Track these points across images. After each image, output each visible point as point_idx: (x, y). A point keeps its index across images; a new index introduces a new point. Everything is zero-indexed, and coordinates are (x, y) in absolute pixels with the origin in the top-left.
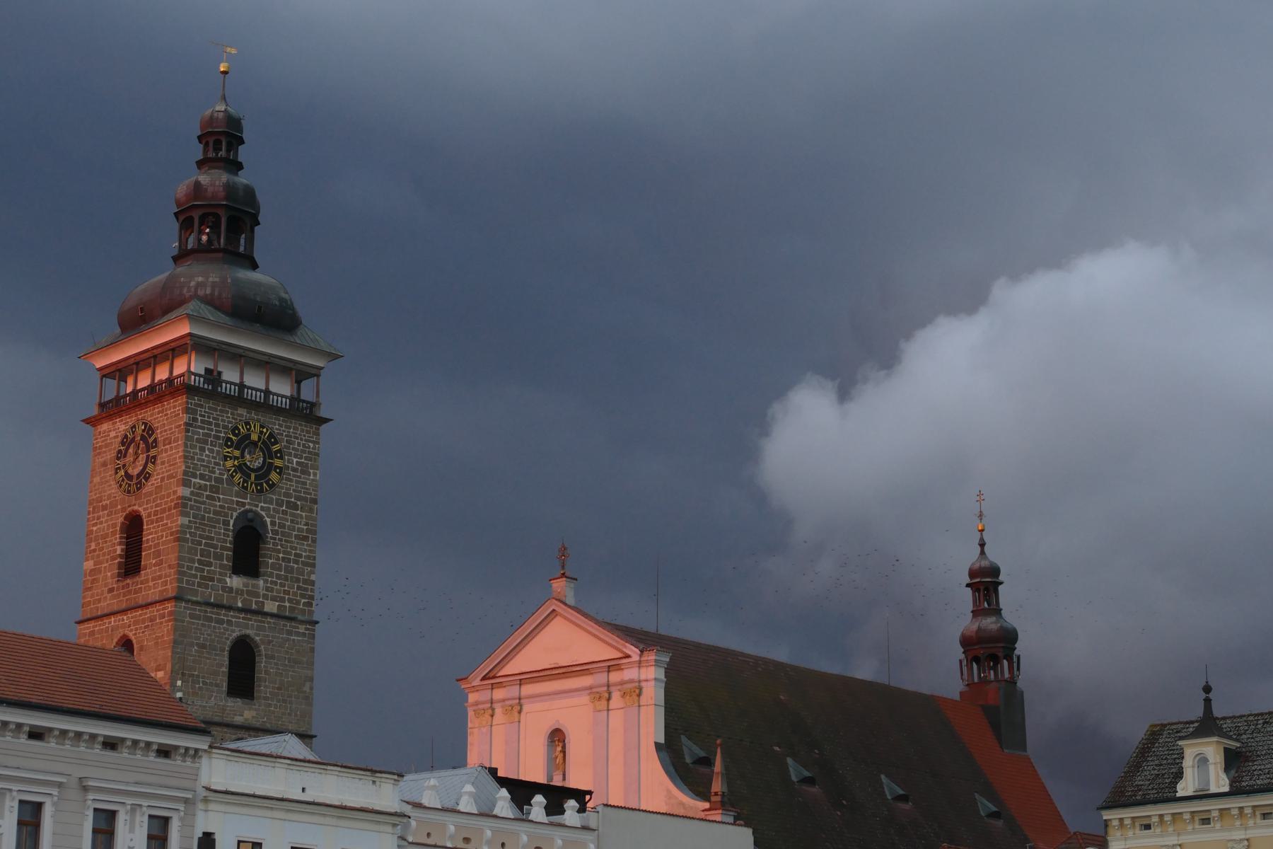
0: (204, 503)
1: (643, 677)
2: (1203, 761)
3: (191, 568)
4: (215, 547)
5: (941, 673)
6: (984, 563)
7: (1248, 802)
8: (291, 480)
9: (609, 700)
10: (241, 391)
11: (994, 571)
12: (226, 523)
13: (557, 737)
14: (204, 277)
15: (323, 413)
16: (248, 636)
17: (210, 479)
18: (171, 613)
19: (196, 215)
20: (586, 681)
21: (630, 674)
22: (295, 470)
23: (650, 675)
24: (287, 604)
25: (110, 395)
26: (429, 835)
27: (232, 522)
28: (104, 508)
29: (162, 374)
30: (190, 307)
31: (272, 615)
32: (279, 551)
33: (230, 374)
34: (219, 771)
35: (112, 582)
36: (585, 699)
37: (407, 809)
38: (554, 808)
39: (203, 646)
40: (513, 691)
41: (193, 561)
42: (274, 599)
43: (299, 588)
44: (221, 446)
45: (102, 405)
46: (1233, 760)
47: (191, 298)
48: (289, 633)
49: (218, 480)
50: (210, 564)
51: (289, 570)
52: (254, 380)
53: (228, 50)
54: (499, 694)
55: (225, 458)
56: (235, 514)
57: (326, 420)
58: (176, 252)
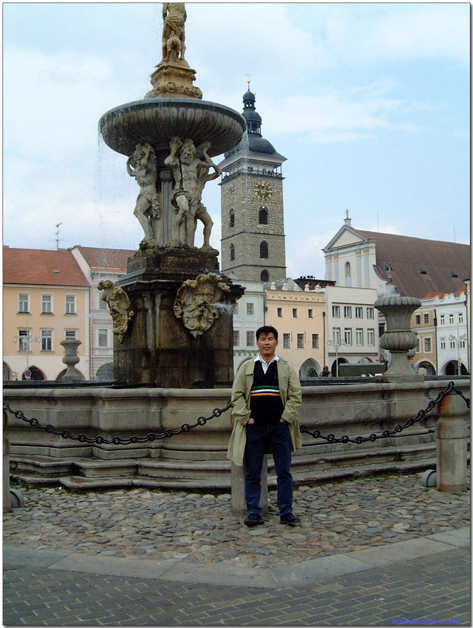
1: (369, 246)
9: (360, 253)
10: (258, 173)
12: (256, 210)
13: (348, 264)
15: (283, 177)
18: (242, 236)
20: (354, 248)
26: (273, 297)
28: (225, 208)
31: (272, 235)
36: (354, 253)
37: (266, 291)
38: (312, 288)
39: (252, 245)
40: (336, 252)
42: (272, 230)
48: (277, 239)
49: (253, 198)
50: (252, 222)
51: (276, 221)
54: (332, 253)
57: (284, 178)
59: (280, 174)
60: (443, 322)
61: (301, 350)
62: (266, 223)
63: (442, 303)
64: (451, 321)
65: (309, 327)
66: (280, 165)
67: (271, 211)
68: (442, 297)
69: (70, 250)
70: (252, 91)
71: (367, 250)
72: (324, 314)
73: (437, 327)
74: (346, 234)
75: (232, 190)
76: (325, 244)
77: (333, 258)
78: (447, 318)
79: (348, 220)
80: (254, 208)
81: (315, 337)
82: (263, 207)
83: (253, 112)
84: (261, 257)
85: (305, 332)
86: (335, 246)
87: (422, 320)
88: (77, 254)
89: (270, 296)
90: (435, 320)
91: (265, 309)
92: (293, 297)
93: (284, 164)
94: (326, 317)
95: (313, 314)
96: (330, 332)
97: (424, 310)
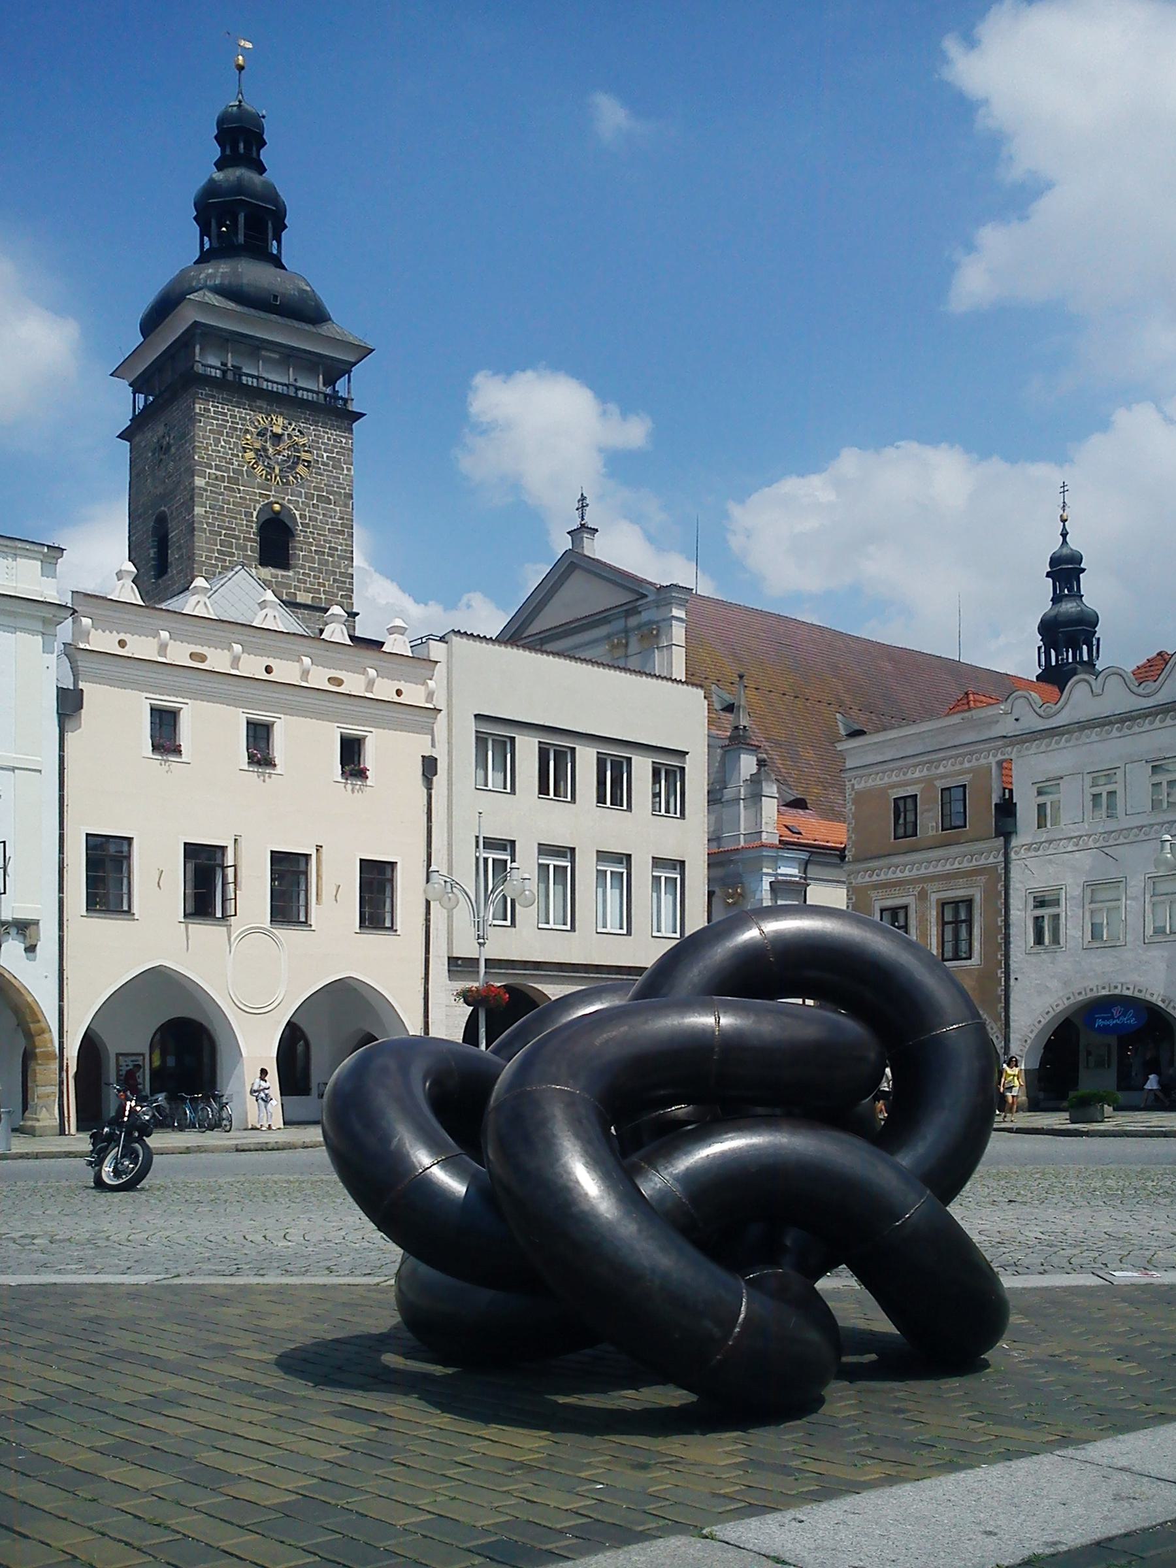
0: (222, 494)
3: (210, 558)
4: (237, 538)
6: (1065, 551)
8: (321, 475)
11: (1076, 559)
15: (354, 407)
17: (227, 470)
20: (603, 631)
21: (645, 616)
22: (324, 464)
24: (323, 596)
27: (255, 514)
28: (140, 516)
32: (311, 544)
41: (213, 551)
42: (307, 591)
43: (335, 580)
44: (238, 437)
47: (201, 289)
49: (237, 472)
53: (242, 43)
55: (244, 450)
56: (258, 506)
58: (197, 255)
61: (286, 934)
62: (286, 567)
66: (345, 369)
67: (307, 525)
73: (1014, 842)
80: (240, 505)
81: (376, 880)
82: (277, 507)
85: (319, 848)
87: (929, 822)
94: (439, 781)
95: (370, 758)
97: (942, 770)
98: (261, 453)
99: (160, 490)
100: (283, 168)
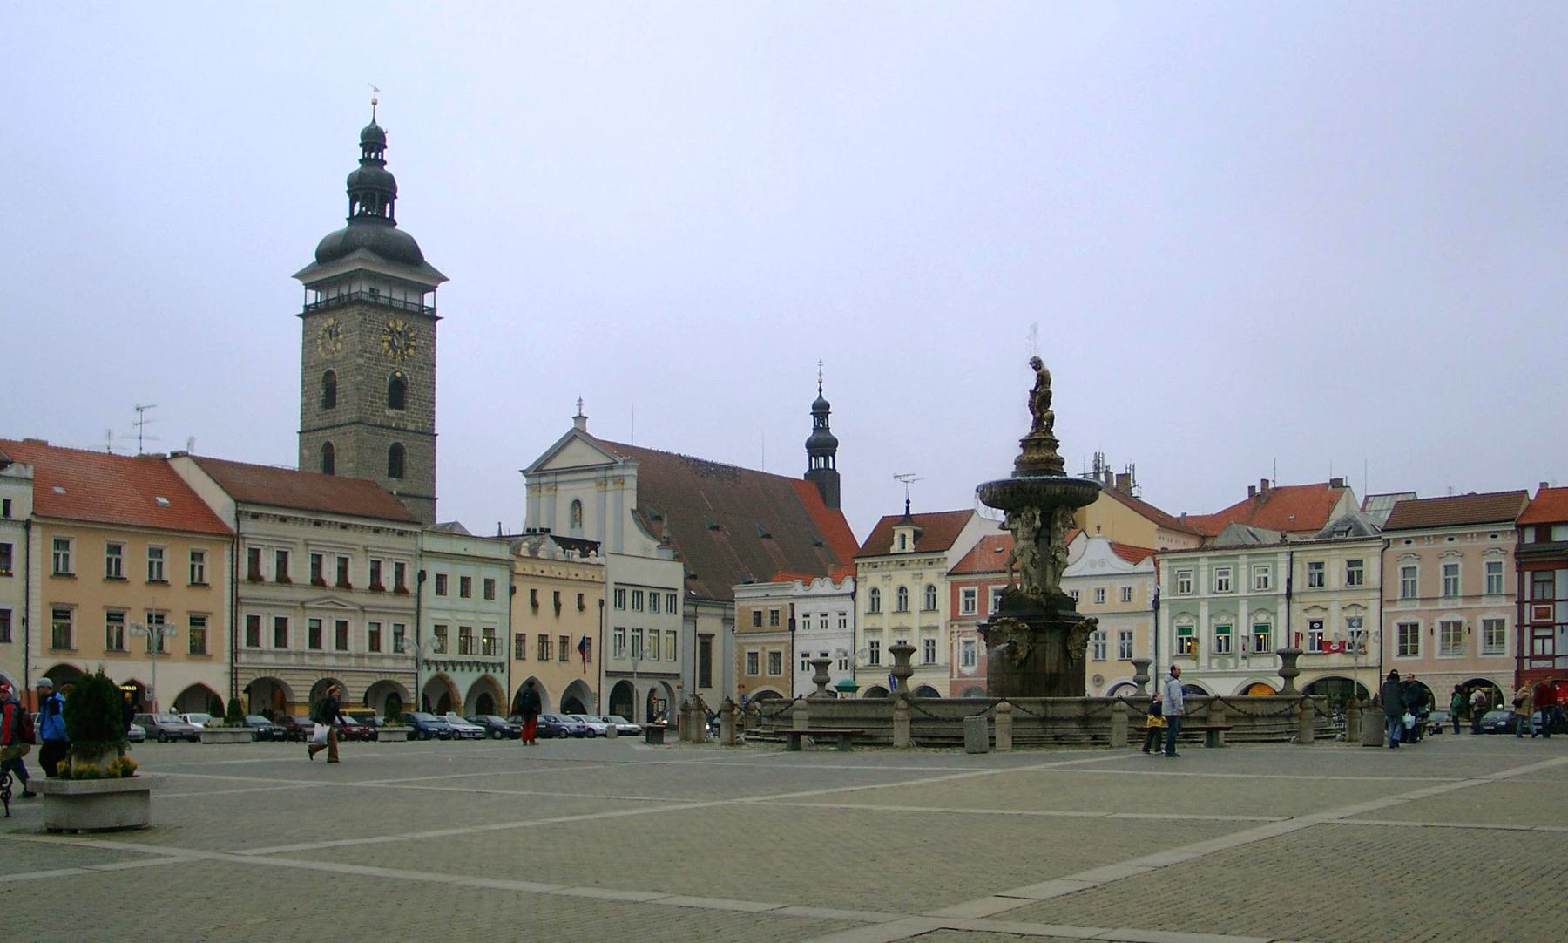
2: (903, 537)
5: (795, 465)
7: (923, 557)
13: (577, 504)
14: (367, 232)
16: (397, 444)
19: (360, 194)
20: (593, 475)
21: (617, 472)
23: (631, 473)
25: (311, 301)
29: (345, 291)
30: (359, 254)
33: (384, 292)
34: (430, 543)
35: (319, 411)
36: (592, 484)
38: (584, 554)
40: (551, 478)
45: (306, 307)
46: (917, 535)
52: (398, 296)
54: (544, 479)
59: (433, 309)
60: (807, 625)
62: (402, 408)
63: (812, 592)
64: (824, 624)
65: (576, 625)
66: (433, 289)
68: (807, 583)
69: (163, 459)
70: (379, 123)
71: (620, 481)
72: (602, 603)
74: (577, 446)
75: (332, 332)
76: (527, 463)
77: (544, 489)
78: (815, 620)
79: (580, 418)
83: (377, 169)
84: (391, 475)
86: (550, 466)
87: (767, 620)
88: (182, 468)
89: (520, 567)
90: (792, 621)
91: (512, 590)
92: (556, 570)
93: (441, 286)
96: (610, 633)
98: (391, 343)
99: (329, 357)
100: (394, 161)
